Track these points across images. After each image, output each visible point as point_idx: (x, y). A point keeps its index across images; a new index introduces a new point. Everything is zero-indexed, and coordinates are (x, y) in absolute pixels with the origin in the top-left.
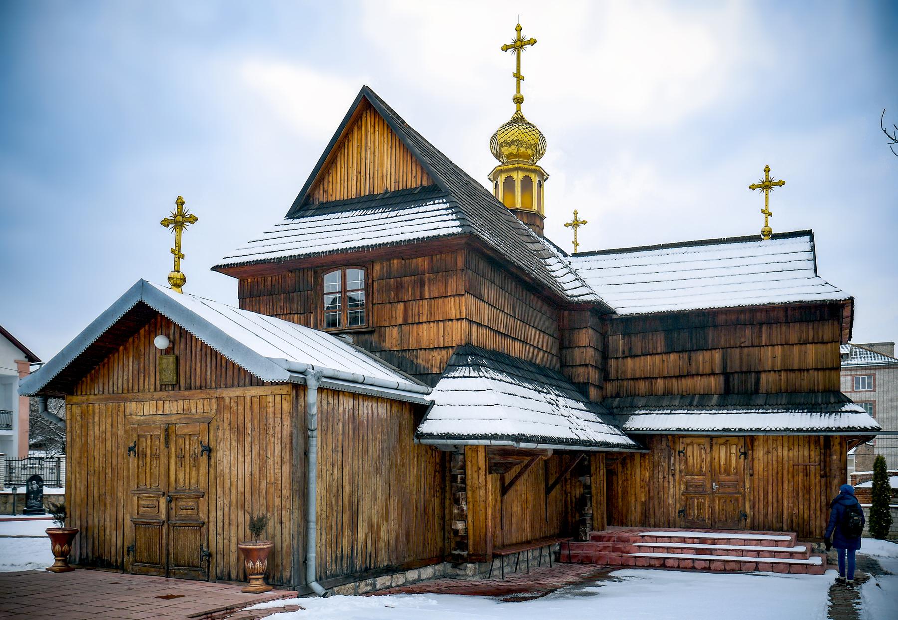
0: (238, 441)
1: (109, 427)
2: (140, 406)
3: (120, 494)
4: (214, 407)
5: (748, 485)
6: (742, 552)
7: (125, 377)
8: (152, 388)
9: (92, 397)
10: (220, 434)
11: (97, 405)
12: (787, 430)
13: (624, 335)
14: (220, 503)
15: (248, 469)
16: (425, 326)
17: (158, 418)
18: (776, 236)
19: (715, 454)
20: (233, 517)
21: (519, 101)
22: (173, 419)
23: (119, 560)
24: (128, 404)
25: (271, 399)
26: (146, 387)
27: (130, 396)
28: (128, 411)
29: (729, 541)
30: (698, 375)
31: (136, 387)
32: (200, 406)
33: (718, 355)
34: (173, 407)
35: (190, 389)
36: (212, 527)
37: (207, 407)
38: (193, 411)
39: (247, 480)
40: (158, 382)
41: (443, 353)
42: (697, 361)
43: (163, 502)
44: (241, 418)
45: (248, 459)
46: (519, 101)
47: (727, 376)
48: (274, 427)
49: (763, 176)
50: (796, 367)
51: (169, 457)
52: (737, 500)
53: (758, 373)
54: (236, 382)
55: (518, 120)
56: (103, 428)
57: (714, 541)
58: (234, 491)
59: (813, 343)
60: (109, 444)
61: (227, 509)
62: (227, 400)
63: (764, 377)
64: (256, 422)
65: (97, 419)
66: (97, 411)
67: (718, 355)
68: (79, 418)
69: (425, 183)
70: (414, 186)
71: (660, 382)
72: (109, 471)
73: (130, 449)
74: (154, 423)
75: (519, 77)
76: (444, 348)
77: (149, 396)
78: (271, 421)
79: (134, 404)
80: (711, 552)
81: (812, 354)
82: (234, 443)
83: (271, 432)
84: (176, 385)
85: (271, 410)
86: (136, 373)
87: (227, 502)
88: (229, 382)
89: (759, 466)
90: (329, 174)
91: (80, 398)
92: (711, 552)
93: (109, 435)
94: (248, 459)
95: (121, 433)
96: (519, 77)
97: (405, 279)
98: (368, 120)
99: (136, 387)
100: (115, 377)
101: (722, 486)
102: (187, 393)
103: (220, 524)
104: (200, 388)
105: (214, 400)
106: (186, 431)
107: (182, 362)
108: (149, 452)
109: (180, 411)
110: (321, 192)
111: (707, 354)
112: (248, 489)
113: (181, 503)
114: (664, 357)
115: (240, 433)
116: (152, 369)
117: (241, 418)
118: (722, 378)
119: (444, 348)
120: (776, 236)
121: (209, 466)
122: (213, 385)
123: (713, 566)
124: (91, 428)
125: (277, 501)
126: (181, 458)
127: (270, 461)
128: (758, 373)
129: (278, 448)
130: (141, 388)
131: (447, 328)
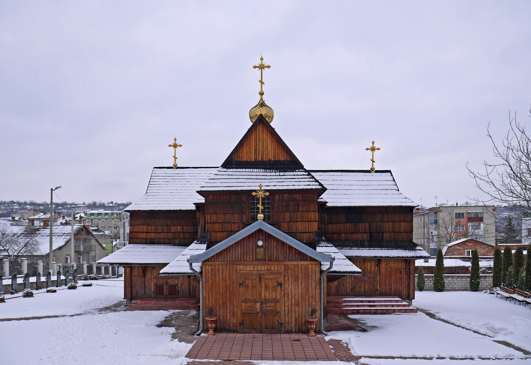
0: (295, 281)
1: (228, 275)
2: (245, 267)
3: (234, 302)
4: (283, 268)
6: (386, 306)
7: (236, 255)
8: (251, 260)
9: (217, 263)
10: (286, 278)
11: (220, 266)
12: (398, 257)
13: (328, 214)
15: (300, 291)
16: (300, 223)
17: (255, 272)
18: (377, 172)
19: (366, 265)
20: (293, 309)
21: (262, 94)
22: (262, 273)
23: (235, 329)
24: (238, 266)
25: (310, 266)
26: (248, 259)
27: (240, 263)
28: (238, 269)
29: (379, 301)
30: (359, 232)
31: (242, 259)
32: (276, 268)
33: (367, 225)
34: (263, 268)
35: (271, 261)
36: (282, 313)
37: (279, 268)
38: (273, 269)
39: (300, 295)
40: (254, 258)
41: (308, 234)
43: (258, 305)
44: (296, 273)
45: (300, 288)
46: (262, 94)
47: (371, 233)
48: (312, 276)
49: (371, 145)
50: (397, 231)
51: (261, 287)
52: (374, 284)
54: (294, 259)
55: (262, 104)
56: (224, 275)
57: (374, 302)
58: (293, 300)
59: (404, 222)
60: (228, 282)
61: (290, 306)
62: (290, 266)
63: (385, 234)
64: (303, 274)
65: (221, 272)
66: (221, 268)
67: (367, 225)
68: (210, 271)
69: (288, 159)
70: (283, 160)
71: (343, 235)
72: (228, 293)
73: (240, 284)
74: (253, 274)
75: (262, 82)
76: (309, 232)
77: (250, 263)
78: (310, 274)
79: (241, 266)
80: (374, 306)
82: (293, 282)
83: (310, 278)
84: (264, 260)
85: (310, 270)
86: (242, 254)
87: (290, 304)
88: (290, 259)
89: (383, 270)
90: (240, 148)
91: (211, 263)
92: (374, 306)
93: (228, 278)
94: (300, 288)
95: (235, 277)
96: (262, 82)
97: (290, 203)
98: (260, 128)
99: (242, 259)
100: (231, 255)
101: (368, 278)
102: (269, 263)
103: (286, 312)
104: (276, 261)
105: (283, 266)
106: (269, 277)
107: (266, 250)
108: (250, 285)
109: (266, 269)
110: (236, 156)
111: (363, 224)
112: (300, 298)
113: (268, 305)
114: (345, 224)
115: (296, 278)
116: (251, 252)
117: (296, 273)
118: (369, 234)
119: (309, 232)
120: (377, 172)
121: (281, 290)
122: (282, 260)
123: (377, 312)
124: (217, 275)
125: (314, 303)
126: (266, 287)
127: (310, 288)
129: (314, 284)
130: (245, 259)
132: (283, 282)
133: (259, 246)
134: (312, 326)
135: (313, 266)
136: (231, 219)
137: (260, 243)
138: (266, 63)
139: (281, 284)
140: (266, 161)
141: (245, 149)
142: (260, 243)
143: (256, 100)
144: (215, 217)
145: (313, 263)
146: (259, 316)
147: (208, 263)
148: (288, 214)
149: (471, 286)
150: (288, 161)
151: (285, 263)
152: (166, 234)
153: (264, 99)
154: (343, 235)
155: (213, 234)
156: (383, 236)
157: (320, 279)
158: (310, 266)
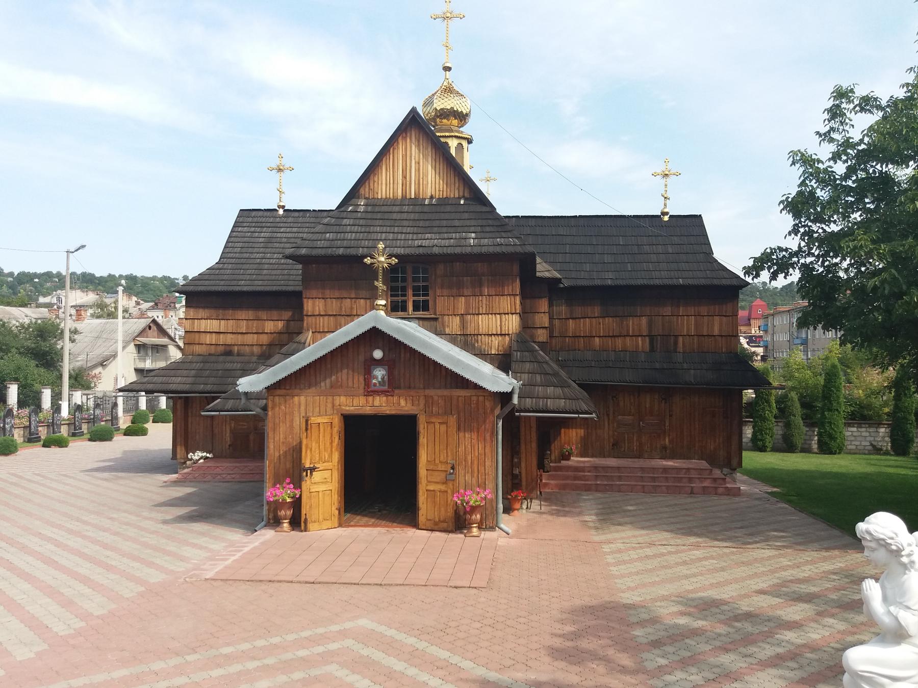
5: (667, 424)
24: (337, 398)
28: (337, 403)
33: (644, 320)
42: (628, 326)
47: (652, 338)
53: (676, 336)
62: (436, 398)
79: (343, 399)
81: (717, 326)
104: (410, 388)
105: (422, 399)
111: (635, 319)
114: (601, 320)
118: (647, 339)
128: (676, 336)
131: (504, 320)
134: (474, 517)
135: (481, 398)
136: (352, 308)
137: (378, 354)
142: (378, 354)
143: (437, 81)
145: (480, 393)
147: (279, 392)
149: (893, 441)
151: (427, 392)
152: (256, 336)
154: (597, 339)
156: (676, 343)
158: (474, 398)
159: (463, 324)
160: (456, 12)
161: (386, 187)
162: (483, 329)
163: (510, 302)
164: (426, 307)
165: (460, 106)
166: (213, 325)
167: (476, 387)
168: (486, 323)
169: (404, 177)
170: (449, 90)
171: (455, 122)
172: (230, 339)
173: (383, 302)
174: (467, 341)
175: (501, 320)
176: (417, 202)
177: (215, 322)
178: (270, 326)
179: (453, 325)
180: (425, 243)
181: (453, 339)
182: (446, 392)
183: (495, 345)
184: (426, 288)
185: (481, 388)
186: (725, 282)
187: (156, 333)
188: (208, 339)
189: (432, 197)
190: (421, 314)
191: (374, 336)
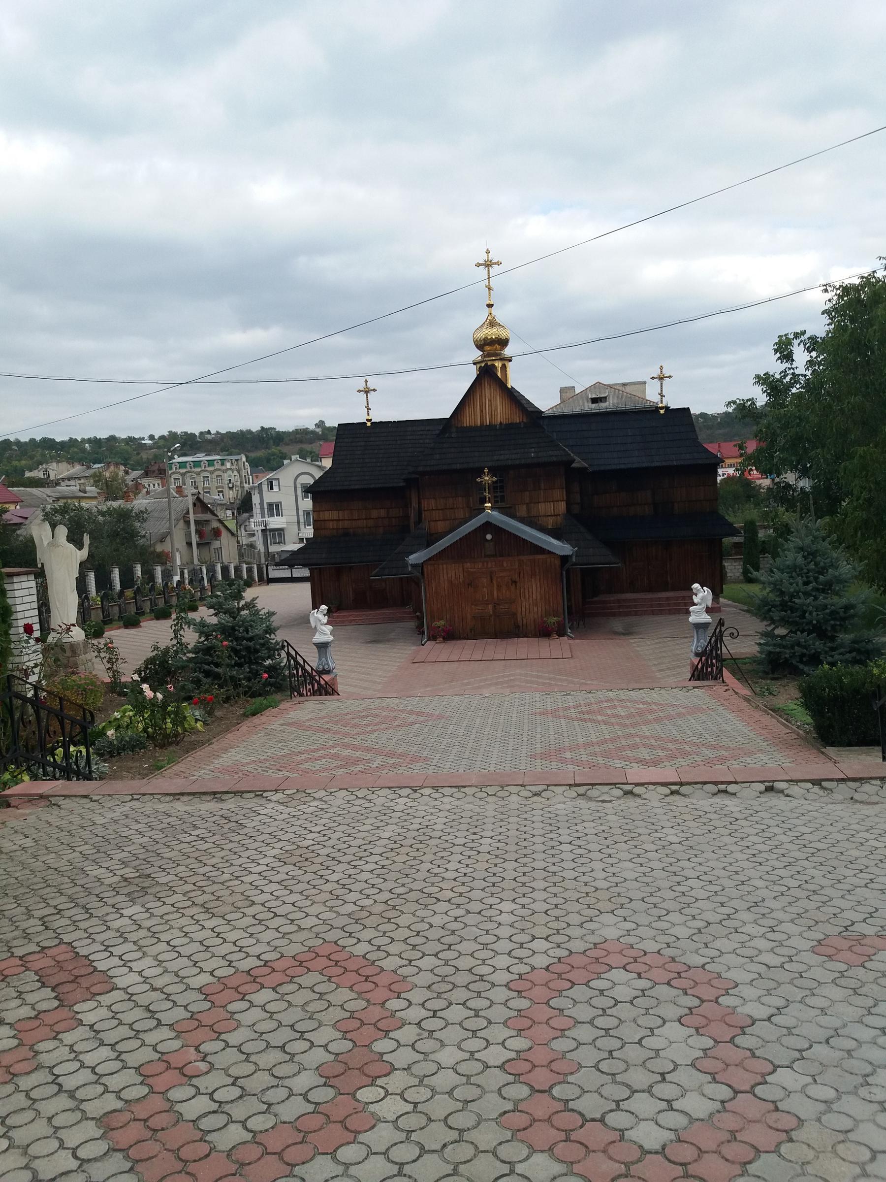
10: (522, 575)
14: (523, 604)
43: (490, 607)
126: (499, 587)
132: (517, 580)
133: (487, 540)
137: (489, 537)
138: (494, 257)
139: (515, 582)
140: (496, 426)
141: (467, 411)
142: (489, 537)
143: (482, 316)
144: (433, 502)
146: (492, 619)
148: (527, 493)
150: (525, 423)
153: (494, 314)
155: (432, 523)
157: (562, 574)
158: (548, 560)
159: (528, 510)
160: (495, 261)
161: (471, 419)
162: (542, 512)
163: (559, 494)
164: (502, 499)
165: (503, 334)
166: (334, 515)
167: (550, 552)
168: (544, 508)
169: (481, 411)
170: (492, 323)
171: (498, 347)
172: (346, 524)
173: (490, 505)
174: (531, 522)
175: (554, 507)
176: (491, 427)
177: (335, 513)
178: (375, 514)
179: (522, 511)
180: (502, 457)
181: (522, 520)
182: (531, 557)
183: (550, 522)
184: (502, 487)
185: (552, 553)
186: (708, 462)
187: (200, 509)
188: (331, 525)
189: (501, 423)
190: (499, 505)
191: (488, 526)
